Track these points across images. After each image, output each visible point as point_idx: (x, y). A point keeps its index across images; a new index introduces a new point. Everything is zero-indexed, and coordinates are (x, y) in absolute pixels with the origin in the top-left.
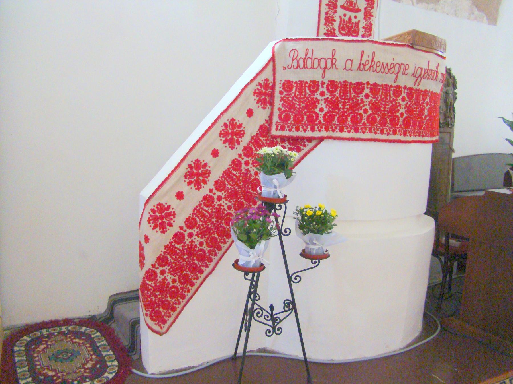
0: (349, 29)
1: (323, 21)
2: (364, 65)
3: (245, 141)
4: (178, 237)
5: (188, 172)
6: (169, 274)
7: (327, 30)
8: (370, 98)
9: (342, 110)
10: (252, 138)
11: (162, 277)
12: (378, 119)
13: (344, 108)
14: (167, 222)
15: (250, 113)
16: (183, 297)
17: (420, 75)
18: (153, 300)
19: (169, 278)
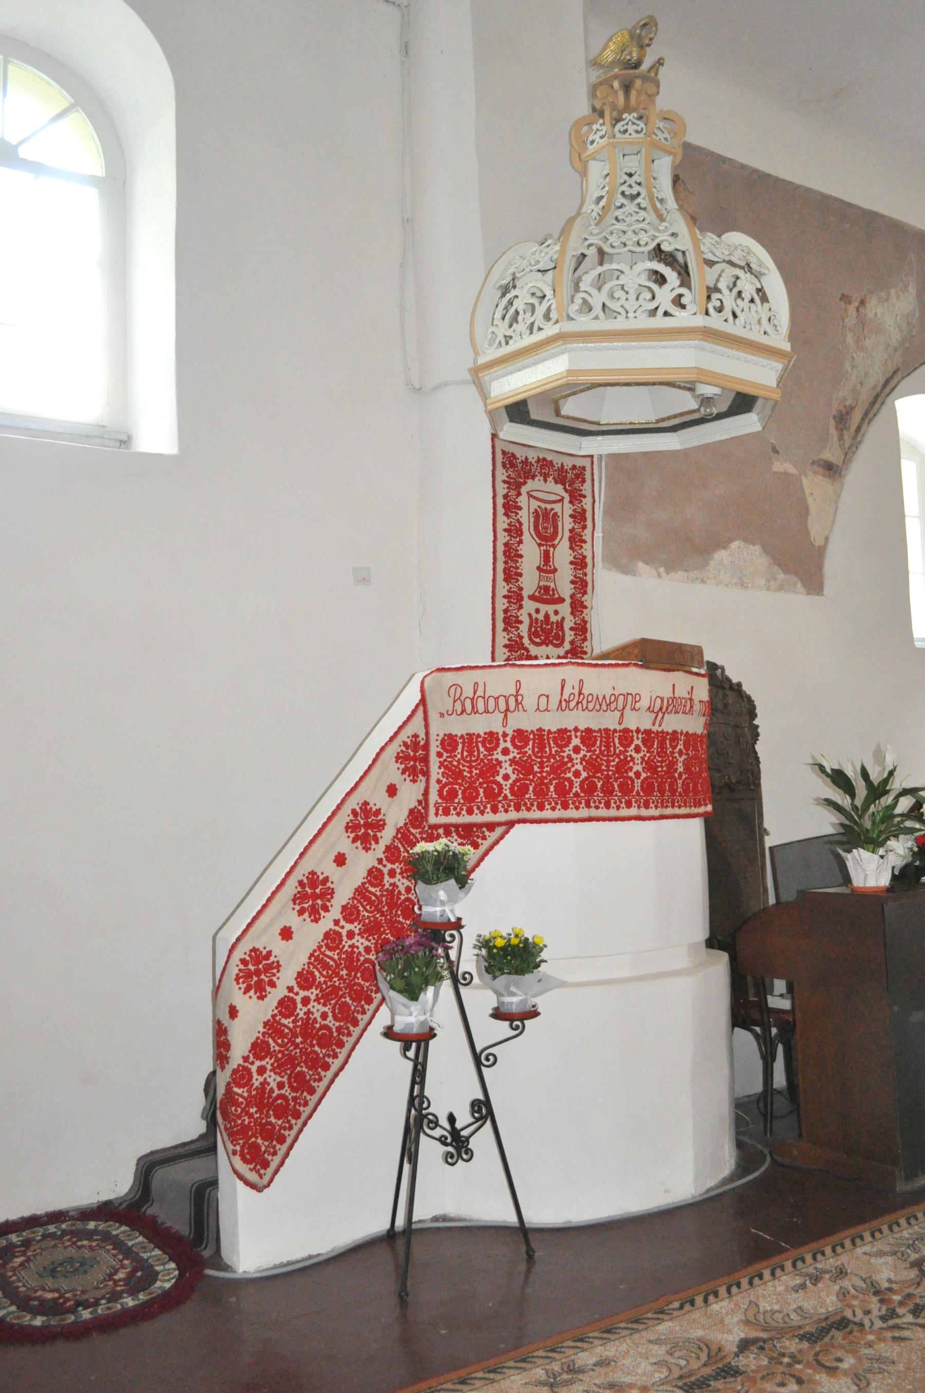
1: (500, 625)
2: (568, 702)
3: (387, 836)
4: (286, 1006)
5: (299, 892)
6: (272, 1074)
7: (509, 640)
8: (582, 753)
9: (539, 775)
10: (398, 830)
11: (261, 1079)
12: (599, 785)
13: (541, 772)
14: (267, 979)
15: (392, 791)
16: (297, 1115)
17: (661, 709)
18: (246, 1123)
19: (273, 1080)
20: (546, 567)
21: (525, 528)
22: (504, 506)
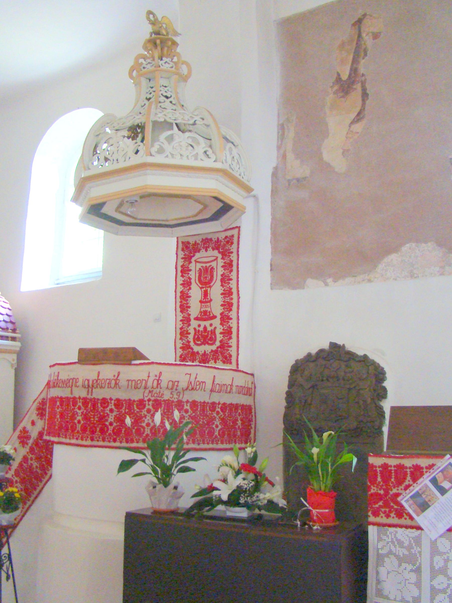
0: (205, 337)
17: (89, 386)
20: (206, 299)
21: (193, 281)
22: (181, 272)
